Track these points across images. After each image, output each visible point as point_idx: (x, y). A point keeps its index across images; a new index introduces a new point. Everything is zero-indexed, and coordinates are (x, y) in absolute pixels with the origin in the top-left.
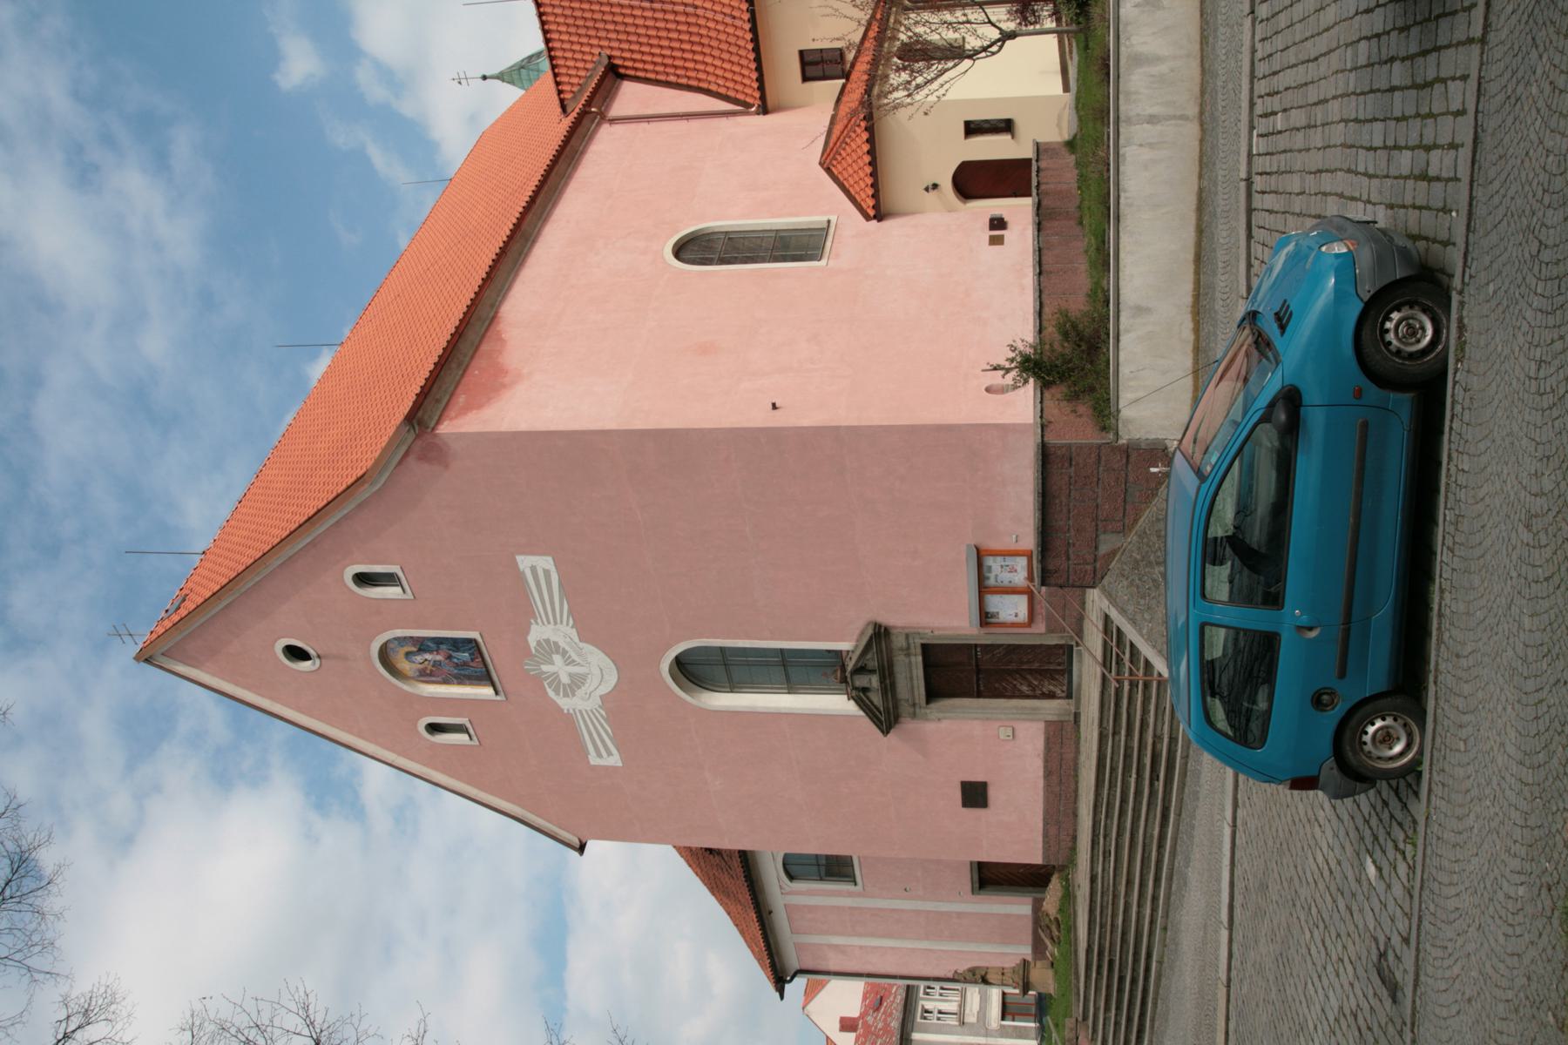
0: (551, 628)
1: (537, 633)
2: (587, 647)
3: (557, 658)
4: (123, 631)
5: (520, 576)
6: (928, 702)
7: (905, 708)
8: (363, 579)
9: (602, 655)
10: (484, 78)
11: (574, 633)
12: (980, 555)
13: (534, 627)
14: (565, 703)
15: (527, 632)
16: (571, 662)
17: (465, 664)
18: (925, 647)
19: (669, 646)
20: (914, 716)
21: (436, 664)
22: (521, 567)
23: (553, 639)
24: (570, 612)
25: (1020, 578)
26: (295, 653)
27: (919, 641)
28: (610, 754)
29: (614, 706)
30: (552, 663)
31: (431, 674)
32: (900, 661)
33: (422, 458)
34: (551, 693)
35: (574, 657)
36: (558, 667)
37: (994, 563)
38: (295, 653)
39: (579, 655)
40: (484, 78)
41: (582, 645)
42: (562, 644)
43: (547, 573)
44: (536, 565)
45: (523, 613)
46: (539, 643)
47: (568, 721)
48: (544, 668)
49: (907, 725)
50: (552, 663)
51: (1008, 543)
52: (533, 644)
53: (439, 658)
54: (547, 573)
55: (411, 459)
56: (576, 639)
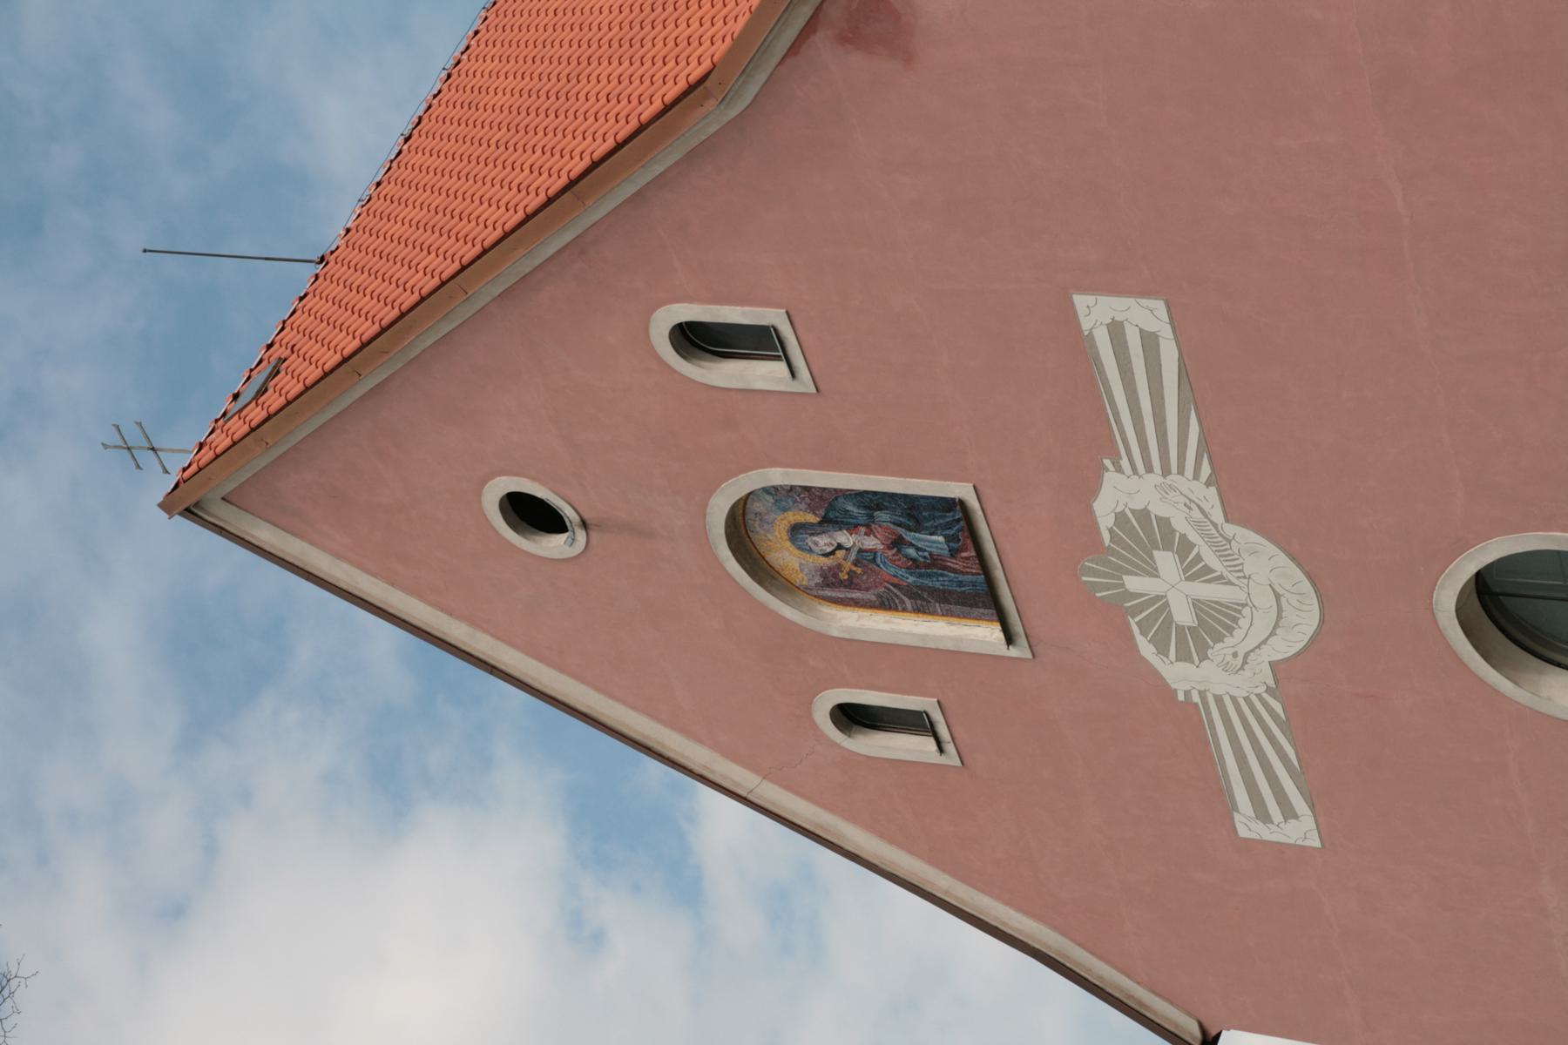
2: (1244, 537)
3: (1166, 561)
4: (135, 438)
5: (1082, 346)
8: (697, 339)
9: (1282, 559)
11: (1211, 499)
13: (1110, 479)
14: (1180, 676)
15: (1094, 491)
17: (935, 562)
19: (1461, 546)
21: (865, 558)
22: (1086, 325)
23: (1159, 509)
24: (1205, 442)
26: (531, 514)
28: (1289, 813)
29: (1310, 693)
30: (1153, 573)
31: (850, 584)
33: (851, 38)
34: (1146, 649)
35: (1210, 559)
36: (1165, 581)
38: (531, 514)
39: (1223, 555)
41: (1230, 529)
42: (1180, 525)
43: (1150, 342)
44: (1123, 321)
45: (1088, 444)
46: (1121, 518)
47: (1186, 722)
48: (1133, 583)
50: (1153, 573)
52: (1105, 521)
53: (871, 543)
54: (1150, 342)
55: (822, 42)
56: (1217, 515)
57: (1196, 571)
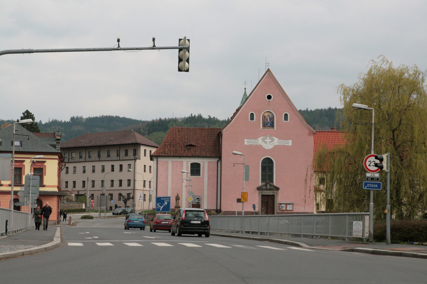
0: (276, 141)
1: (276, 139)
2: (273, 146)
3: (270, 140)
5: (288, 140)
6: (262, 195)
7: (261, 191)
8: (286, 115)
10: (245, 89)
11: (276, 144)
12: (293, 204)
14: (260, 139)
15: (276, 137)
16: (270, 142)
17: (267, 125)
18: (274, 195)
19: (274, 158)
20: (259, 192)
21: (267, 120)
25: (288, 209)
26: (269, 97)
27: (275, 194)
32: (272, 192)
33: (309, 132)
34: (262, 137)
35: (271, 143)
36: (268, 140)
37: (291, 206)
38: (269, 97)
40: (245, 89)
44: (290, 143)
45: (280, 138)
47: (256, 138)
48: (268, 138)
49: (257, 192)
51: (295, 207)
55: (309, 131)
57: (270, 142)
